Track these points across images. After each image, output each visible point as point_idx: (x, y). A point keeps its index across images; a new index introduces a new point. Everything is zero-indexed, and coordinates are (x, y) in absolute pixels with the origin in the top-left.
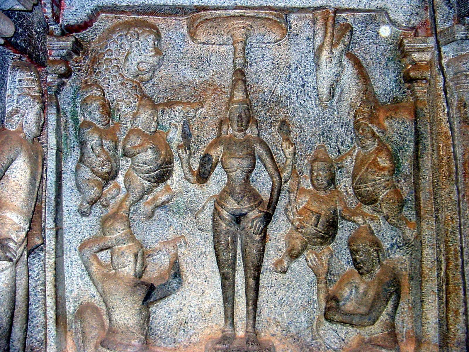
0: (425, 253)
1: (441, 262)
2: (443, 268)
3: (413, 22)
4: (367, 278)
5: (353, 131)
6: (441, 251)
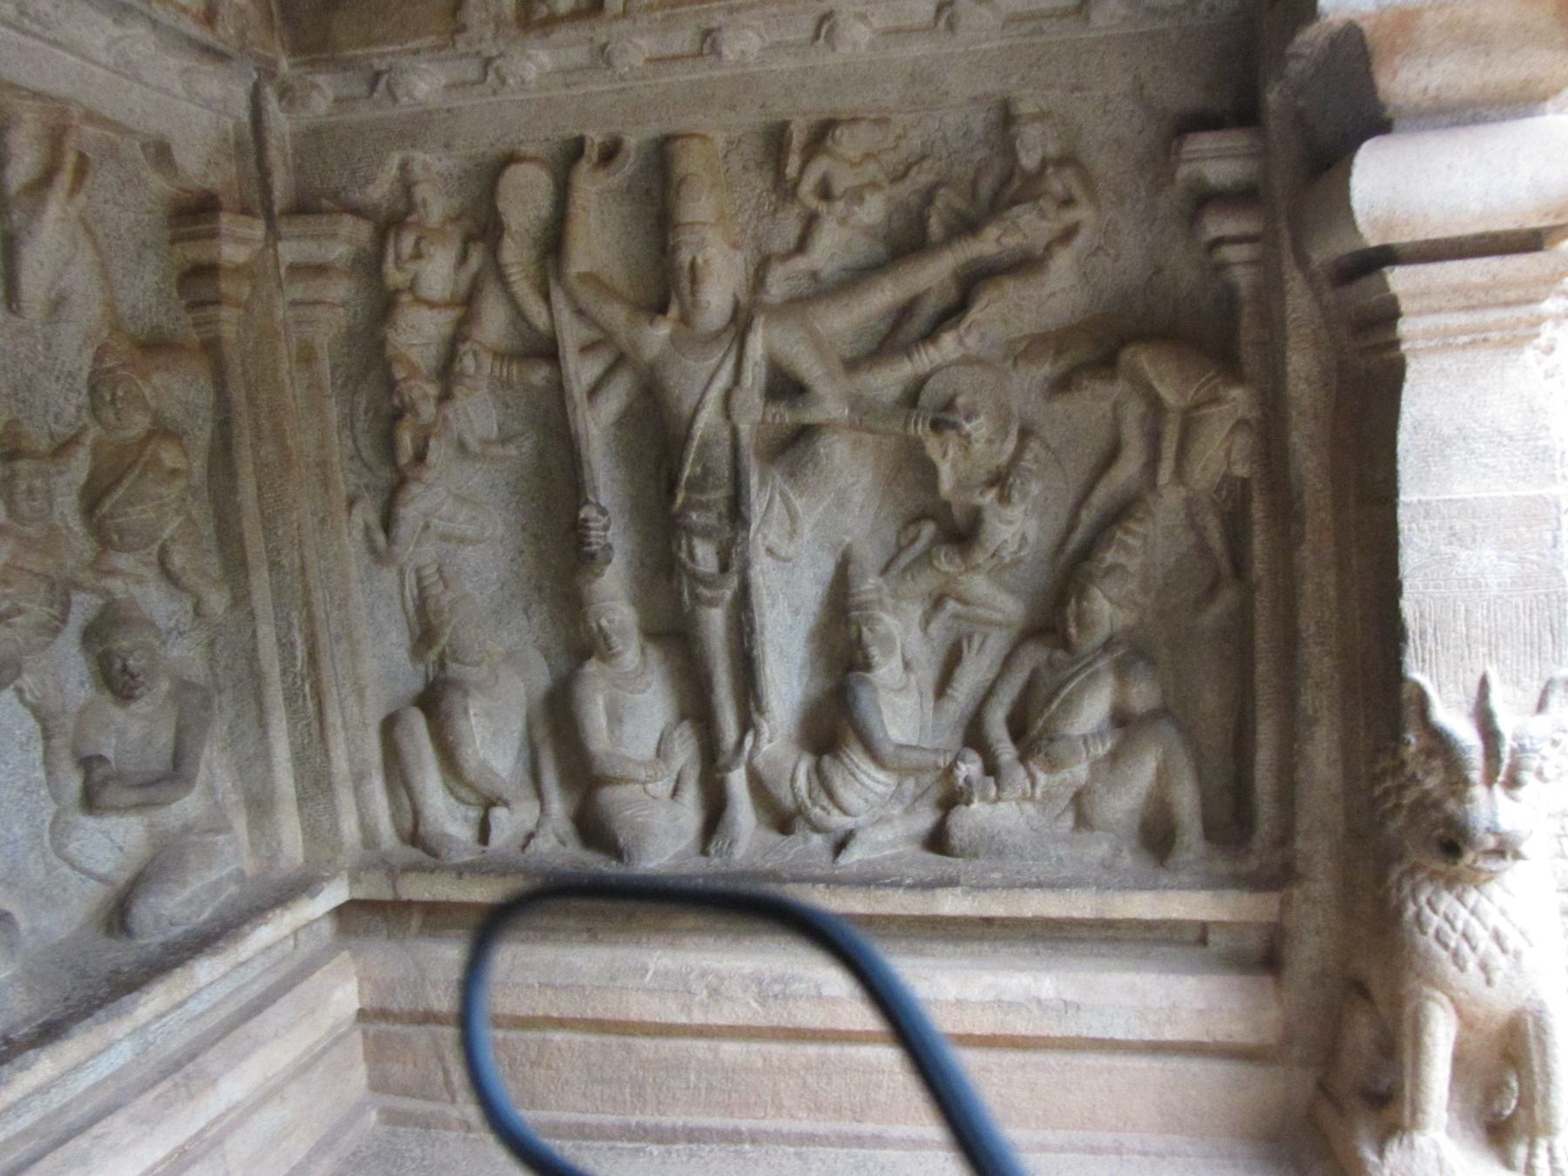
0: (260, 634)
1: (292, 644)
2: (299, 653)
3: (212, 179)
4: (141, 707)
5: (84, 391)
6: (290, 625)
